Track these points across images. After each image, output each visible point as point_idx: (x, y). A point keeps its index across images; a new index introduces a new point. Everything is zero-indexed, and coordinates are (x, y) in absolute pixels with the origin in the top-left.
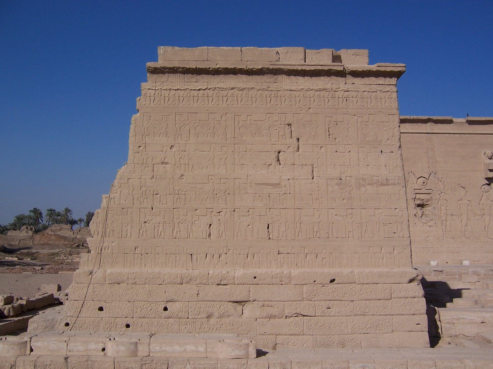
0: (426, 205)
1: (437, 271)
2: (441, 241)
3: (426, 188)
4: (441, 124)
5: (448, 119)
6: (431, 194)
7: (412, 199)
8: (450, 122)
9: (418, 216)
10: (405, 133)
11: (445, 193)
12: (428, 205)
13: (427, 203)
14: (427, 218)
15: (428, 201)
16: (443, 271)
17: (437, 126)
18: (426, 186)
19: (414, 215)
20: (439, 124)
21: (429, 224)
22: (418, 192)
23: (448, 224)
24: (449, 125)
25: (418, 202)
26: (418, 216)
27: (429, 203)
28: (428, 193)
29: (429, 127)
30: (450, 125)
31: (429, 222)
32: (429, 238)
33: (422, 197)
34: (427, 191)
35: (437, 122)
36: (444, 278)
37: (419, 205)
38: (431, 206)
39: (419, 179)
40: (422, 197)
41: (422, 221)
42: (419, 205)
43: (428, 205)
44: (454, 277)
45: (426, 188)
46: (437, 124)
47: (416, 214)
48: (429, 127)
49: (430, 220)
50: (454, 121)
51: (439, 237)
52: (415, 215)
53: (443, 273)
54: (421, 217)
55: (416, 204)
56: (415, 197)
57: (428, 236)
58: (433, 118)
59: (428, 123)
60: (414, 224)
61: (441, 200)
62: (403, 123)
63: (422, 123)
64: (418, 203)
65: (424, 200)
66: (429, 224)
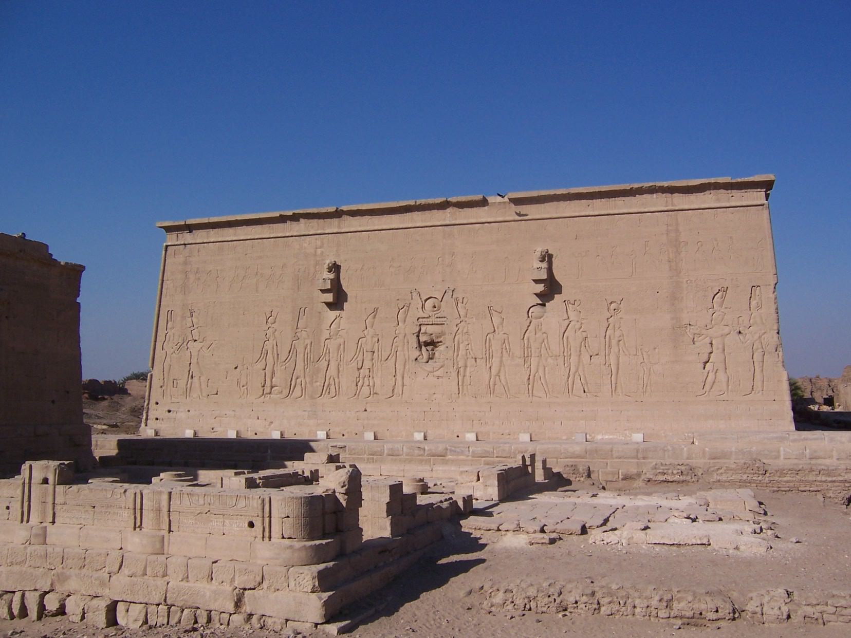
0: (438, 342)
1: (336, 446)
2: (454, 401)
3: (436, 316)
4: (470, 209)
5: (475, 200)
6: (444, 324)
7: (414, 334)
8: (484, 203)
9: (421, 361)
10: (410, 228)
11: (467, 322)
12: (441, 342)
13: (439, 340)
14: (435, 365)
15: (440, 337)
16: (346, 447)
17: (462, 213)
18: (438, 312)
19: (414, 359)
20: (465, 209)
21: (438, 373)
22: (423, 323)
23: (468, 374)
24: (482, 208)
25: (423, 338)
26: (421, 361)
27: (442, 339)
28: (439, 323)
29: (449, 215)
30: (484, 208)
31: (438, 370)
32: (435, 396)
33: (430, 329)
34: (439, 319)
35: (461, 205)
36: (346, 458)
37: (427, 344)
38: (444, 344)
39: (428, 301)
40: (430, 329)
41: (425, 368)
42: (427, 344)
43: (441, 342)
44: (361, 458)
45: (436, 316)
46: (463, 208)
47: (418, 359)
48: (447, 216)
49: (439, 367)
50: (489, 201)
51: (451, 394)
52: (416, 359)
53: (346, 451)
54: (427, 362)
55: (421, 341)
56: (418, 330)
57: (434, 394)
58: (451, 200)
59: (448, 209)
60: (414, 373)
61: (458, 334)
62: (409, 212)
63: (438, 210)
64: (424, 341)
65: (433, 335)
66: (438, 373)
